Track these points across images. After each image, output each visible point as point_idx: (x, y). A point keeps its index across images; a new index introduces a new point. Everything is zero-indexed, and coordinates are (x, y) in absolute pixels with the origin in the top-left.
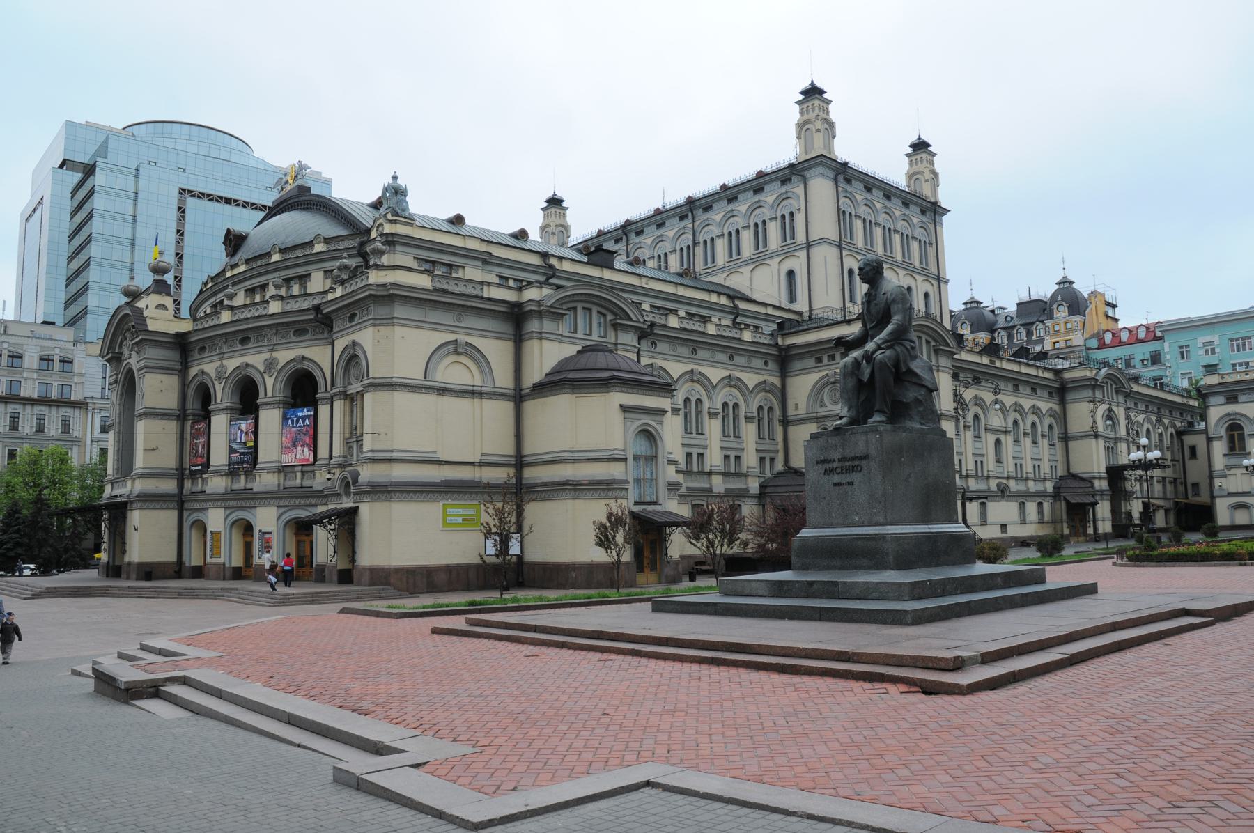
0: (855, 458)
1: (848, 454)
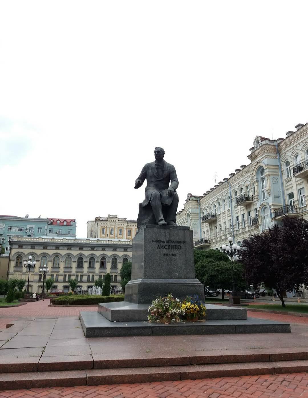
1: (173, 239)
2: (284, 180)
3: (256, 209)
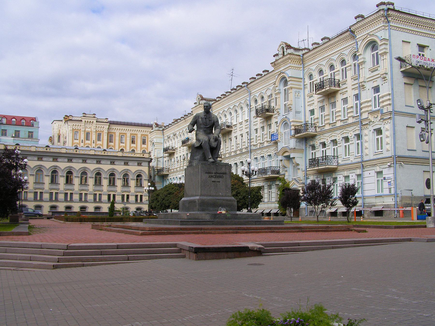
0: (221, 173)
3: (276, 122)
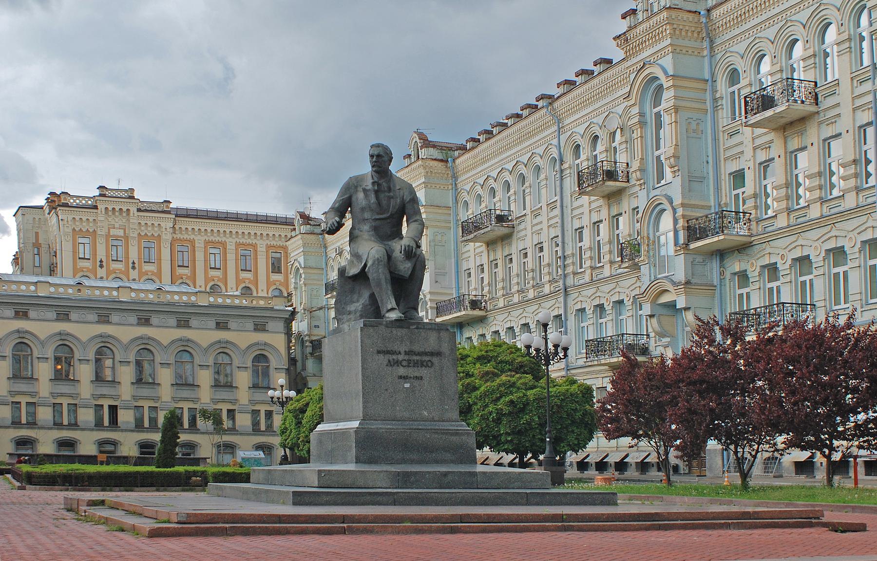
0: (426, 354)
1: (417, 348)
2: (721, 128)
